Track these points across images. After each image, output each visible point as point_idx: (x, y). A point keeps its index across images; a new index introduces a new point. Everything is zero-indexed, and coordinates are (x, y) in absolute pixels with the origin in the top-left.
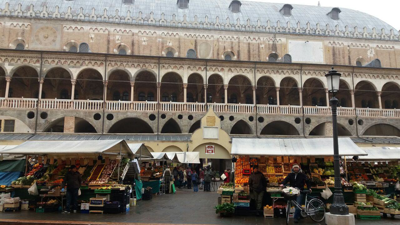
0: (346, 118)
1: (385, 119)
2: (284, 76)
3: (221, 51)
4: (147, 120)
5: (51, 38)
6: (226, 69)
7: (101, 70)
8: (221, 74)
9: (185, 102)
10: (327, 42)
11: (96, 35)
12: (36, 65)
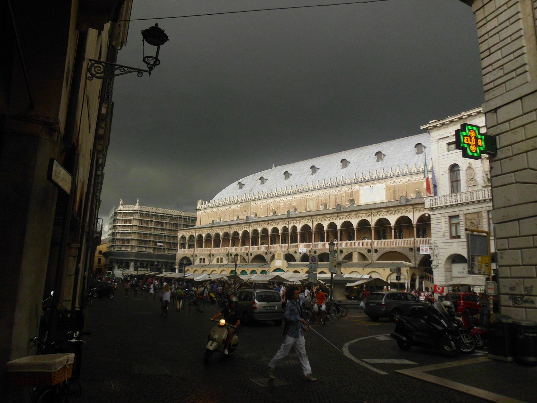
0: (366, 249)
1: (394, 248)
2: (329, 222)
3: (320, 203)
4: (264, 255)
5: (247, 212)
6: (298, 222)
7: (248, 230)
8: (296, 225)
9: (280, 244)
10: (389, 182)
11: (263, 206)
12: (228, 231)
